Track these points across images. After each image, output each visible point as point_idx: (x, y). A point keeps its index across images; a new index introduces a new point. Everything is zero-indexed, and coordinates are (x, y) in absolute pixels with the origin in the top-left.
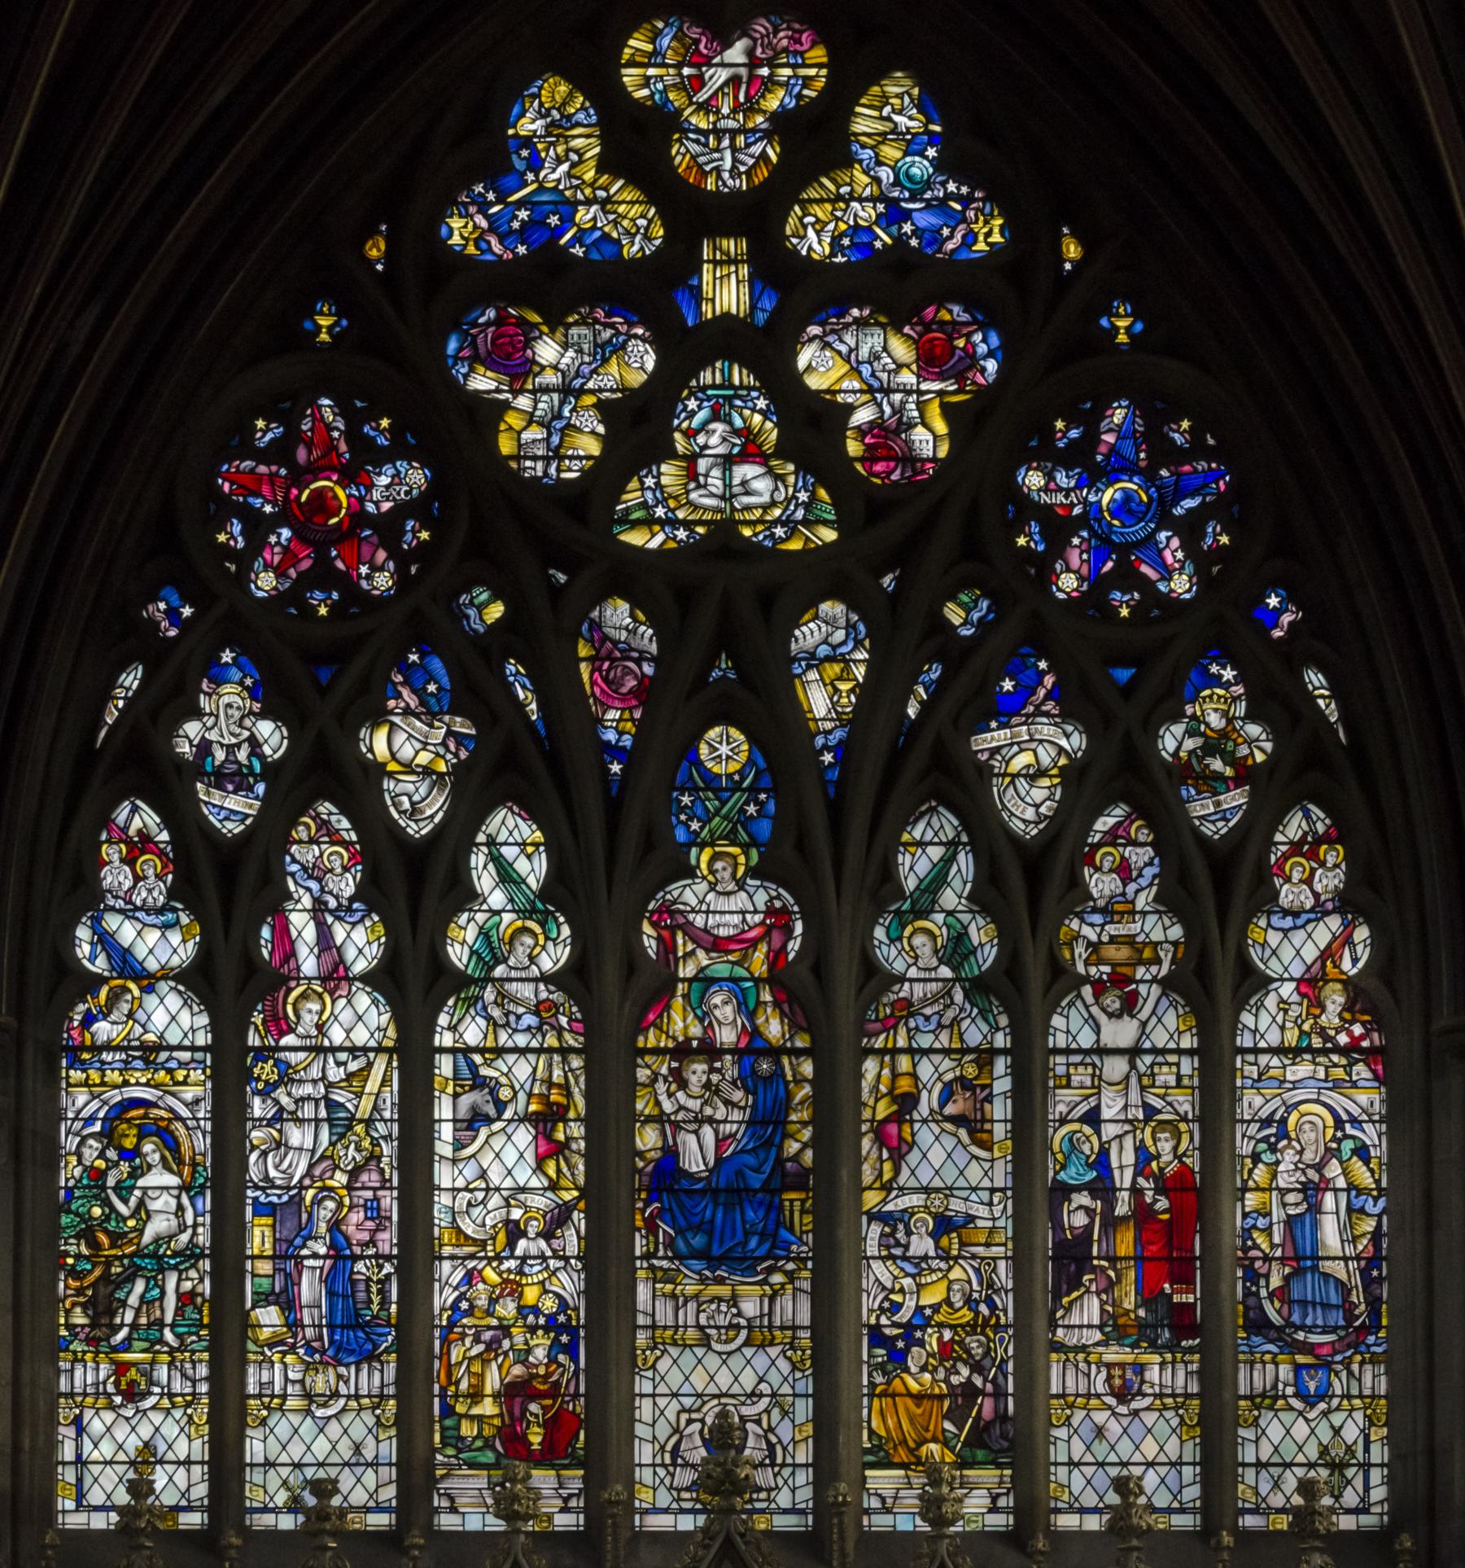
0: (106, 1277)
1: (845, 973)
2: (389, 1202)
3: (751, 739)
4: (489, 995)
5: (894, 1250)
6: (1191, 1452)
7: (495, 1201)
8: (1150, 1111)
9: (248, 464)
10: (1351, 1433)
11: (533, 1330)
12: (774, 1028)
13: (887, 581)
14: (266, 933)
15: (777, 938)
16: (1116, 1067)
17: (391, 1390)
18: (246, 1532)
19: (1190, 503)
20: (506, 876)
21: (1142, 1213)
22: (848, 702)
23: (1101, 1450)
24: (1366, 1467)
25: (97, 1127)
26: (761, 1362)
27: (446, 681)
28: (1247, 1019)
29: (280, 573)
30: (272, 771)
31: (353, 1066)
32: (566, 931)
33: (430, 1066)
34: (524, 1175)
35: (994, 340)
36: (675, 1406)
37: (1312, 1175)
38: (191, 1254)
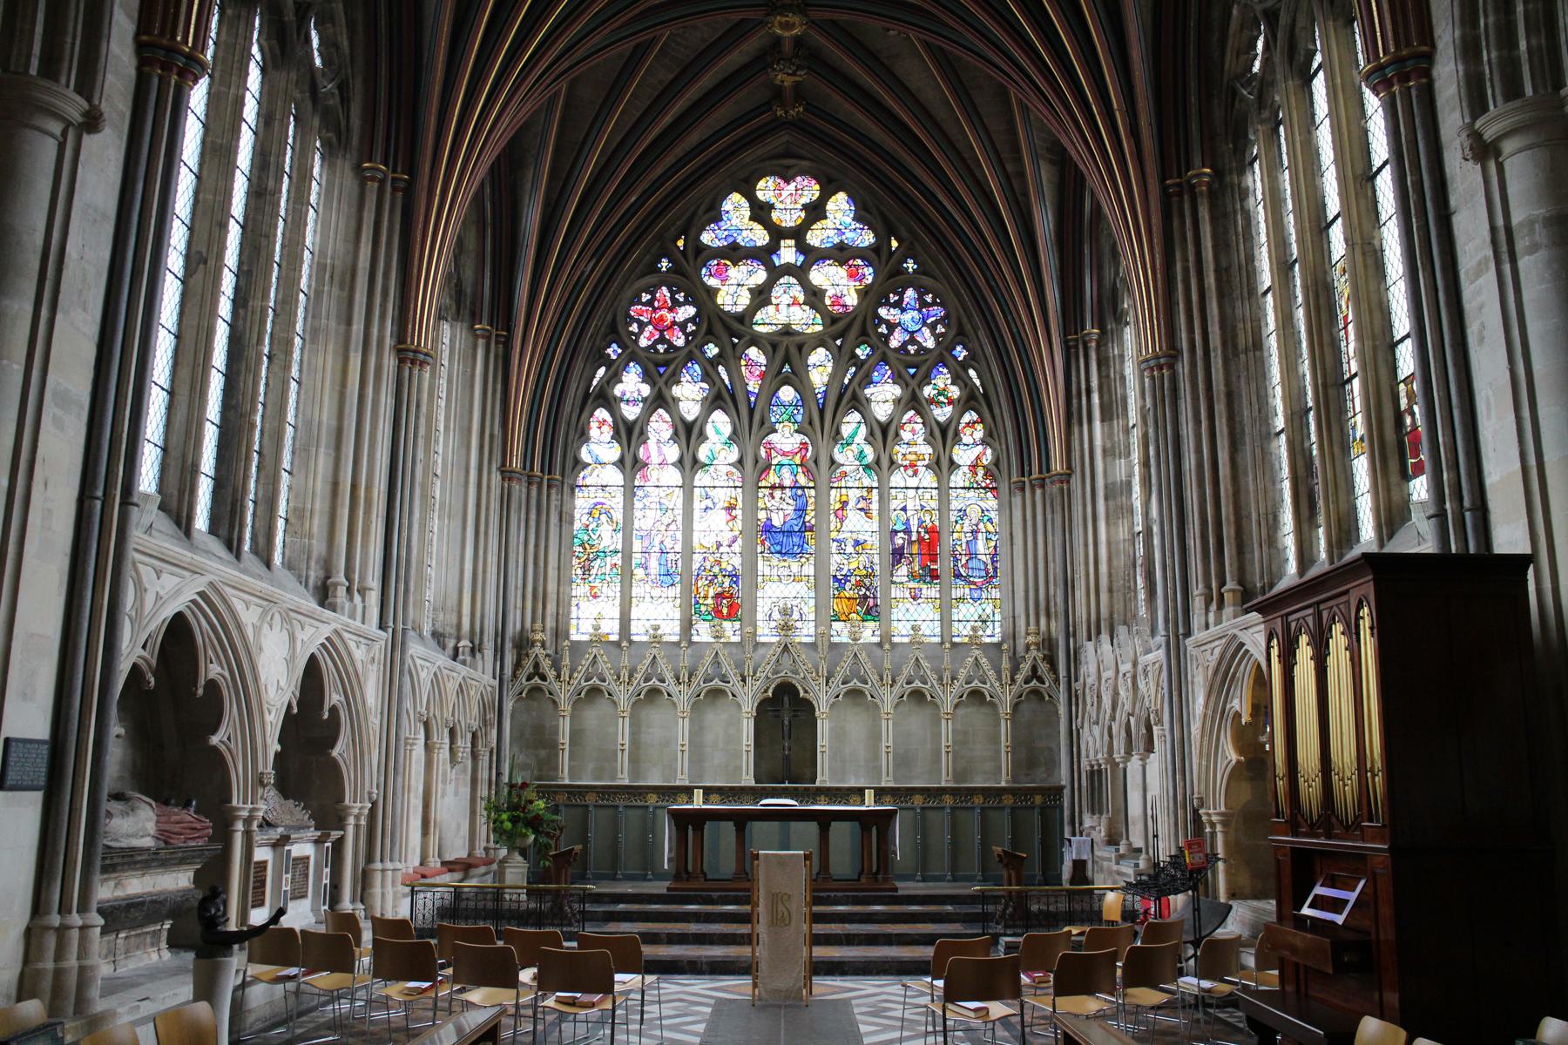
0: (588, 559)
1: (824, 462)
2: (679, 535)
3: (796, 390)
4: (712, 468)
5: (841, 552)
6: (937, 617)
7: (713, 534)
8: (923, 507)
9: (640, 307)
10: (989, 611)
11: (724, 576)
12: (802, 480)
13: (838, 342)
14: (641, 449)
15: (803, 452)
16: (911, 493)
17: (678, 596)
18: (631, 642)
19: (934, 319)
20: (718, 432)
21: (921, 540)
22: (826, 379)
23: (908, 616)
24: (993, 621)
25: (587, 511)
26: (798, 586)
27: (700, 373)
28: (952, 477)
29: (649, 340)
30: (644, 400)
31: (668, 492)
32: (736, 449)
33: (692, 492)
34: (723, 526)
35: (871, 270)
36: (770, 601)
37: (975, 527)
38: (616, 552)
